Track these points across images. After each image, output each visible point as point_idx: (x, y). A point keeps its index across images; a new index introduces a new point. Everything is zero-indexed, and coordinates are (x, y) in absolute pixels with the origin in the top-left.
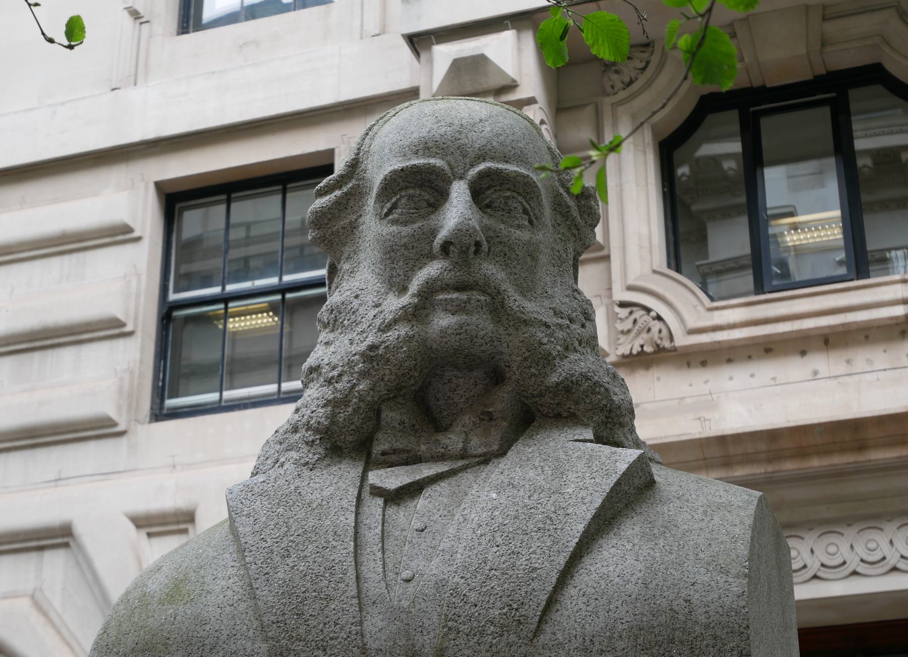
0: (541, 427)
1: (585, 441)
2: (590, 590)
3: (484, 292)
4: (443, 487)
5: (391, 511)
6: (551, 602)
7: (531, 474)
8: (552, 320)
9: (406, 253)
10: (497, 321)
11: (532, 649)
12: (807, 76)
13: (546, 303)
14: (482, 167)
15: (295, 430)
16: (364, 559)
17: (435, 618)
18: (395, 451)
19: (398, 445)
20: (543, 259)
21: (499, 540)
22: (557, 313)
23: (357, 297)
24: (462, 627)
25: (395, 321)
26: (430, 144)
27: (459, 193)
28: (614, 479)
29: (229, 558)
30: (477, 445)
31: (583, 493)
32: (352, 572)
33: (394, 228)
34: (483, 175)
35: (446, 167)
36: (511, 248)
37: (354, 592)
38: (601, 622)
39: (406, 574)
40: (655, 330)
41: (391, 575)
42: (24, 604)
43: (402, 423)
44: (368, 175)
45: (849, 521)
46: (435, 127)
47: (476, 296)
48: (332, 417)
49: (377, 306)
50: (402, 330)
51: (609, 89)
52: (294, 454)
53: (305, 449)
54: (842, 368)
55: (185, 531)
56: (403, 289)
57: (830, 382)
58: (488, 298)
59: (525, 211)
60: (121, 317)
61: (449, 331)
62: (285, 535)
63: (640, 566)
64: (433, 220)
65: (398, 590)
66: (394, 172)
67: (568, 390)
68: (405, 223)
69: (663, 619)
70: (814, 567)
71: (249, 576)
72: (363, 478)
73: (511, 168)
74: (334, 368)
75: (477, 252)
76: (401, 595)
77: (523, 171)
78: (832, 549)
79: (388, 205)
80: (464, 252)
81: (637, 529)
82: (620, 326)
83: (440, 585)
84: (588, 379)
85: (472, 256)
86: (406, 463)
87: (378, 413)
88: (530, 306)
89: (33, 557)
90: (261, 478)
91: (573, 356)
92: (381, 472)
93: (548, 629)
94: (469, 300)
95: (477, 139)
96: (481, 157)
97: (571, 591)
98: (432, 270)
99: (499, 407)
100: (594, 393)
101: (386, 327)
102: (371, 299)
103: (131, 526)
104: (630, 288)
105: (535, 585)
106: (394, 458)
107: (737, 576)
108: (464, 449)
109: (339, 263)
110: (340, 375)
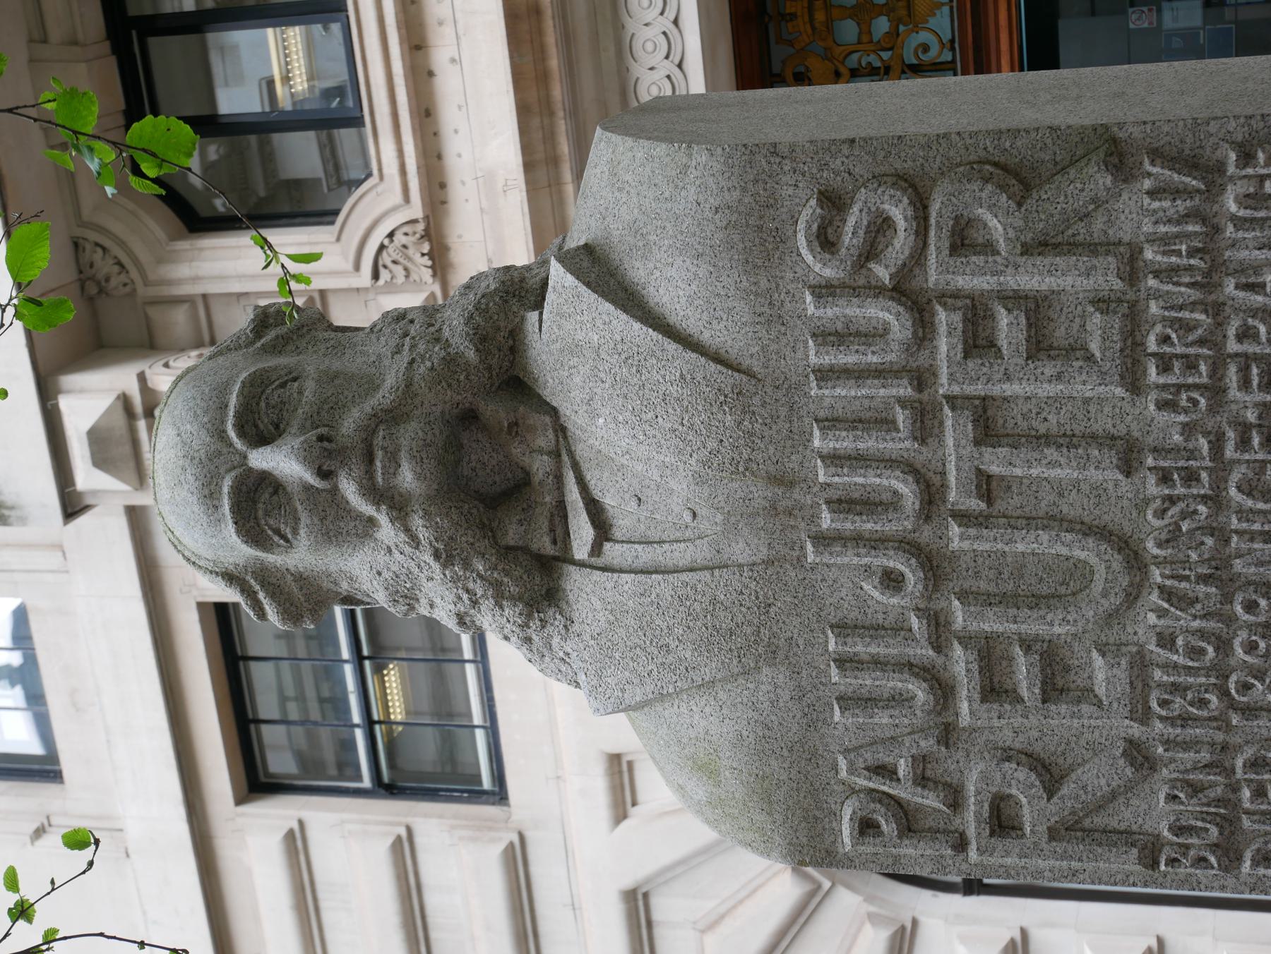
0: (525, 369)
1: (541, 321)
2: (705, 317)
3: (374, 431)
4: (591, 477)
5: (617, 533)
6: (717, 359)
7: (577, 380)
8: (405, 356)
9: (330, 518)
10: (406, 417)
11: (769, 380)
12: (112, 62)
13: (387, 362)
14: (232, 434)
15: (528, 640)
16: (670, 564)
17: (735, 485)
18: (552, 530)
19: (545, 526)
20: (336, 365)
21: (650, 415)
22: (398, 350)
23: (379, 574)
24: (745, 456)
25: (407, 530)
26: (206, 492)
27: (261, 459)
28: (583, 289)
29: (669, 711)
30: (545, 440)
31: (599, 323)
32: (685, 577)
33: (302, 532)
34: (242, 433)
35: (233, 474)
36: (325, 401)
37: (707, 574)
38: (740, 306)
39: (687, 517)
40: (404, 240)
41: (688, 534)
42: (709, 939)
43: (520, 522)
44: (241, 562)
45: (618, 26)
46: (186, 487)
47: (379, 440)
48: (514, 599)
49: (390, 551)
50: (417, 522)
51: (128, 289)
52: (556, 641)
53: (549, 629)
54: (448, 30)
55: (630, 764)
56: (371, 521)
58: (382, 427)
59: (283, 385)
60: (390, 840)
61: (419, 470)
62: (644, 650)
63: (679, 262)
64: (294, 489)
65: (704, 526)
66: (238, 532)
67: (484, 339)
68: (297, 520)
69: (736, 238)
70: (669, 67)
71: (690, 688)
72: (582, 564)
73: (233, 401)
74: (460, 598)
75: (329, 440)
76: (711, 522)
77: (237, 387)
78: (649, 46)
79: (276, 538)
80: (329, 454)
81: (637, 264)
82: (400, 278)
83: (699, 480)
84: (471, 317)
85: (333, 445)
86: (565, 517)
87: (509, 548)
88: (390, 381)
89: (658, 932)
90: (581, 678)
91: (446, 333)
92: (575, 545)
93: (747, 362)
94: (384, 449)
95: (201, 440)
96: (221, 435)
97: (706, 337)
98: (349, 489)
99: (502, 415)
100: (487, 310)
101: (414, 541)
102: (382, 558)
103: (625, 824)
104: (357, 267)
105: (699, 377)
106: (559, 531)
107: (690, 156)
108: (549, 453)
109: (341, 593)
110: (468, 591)
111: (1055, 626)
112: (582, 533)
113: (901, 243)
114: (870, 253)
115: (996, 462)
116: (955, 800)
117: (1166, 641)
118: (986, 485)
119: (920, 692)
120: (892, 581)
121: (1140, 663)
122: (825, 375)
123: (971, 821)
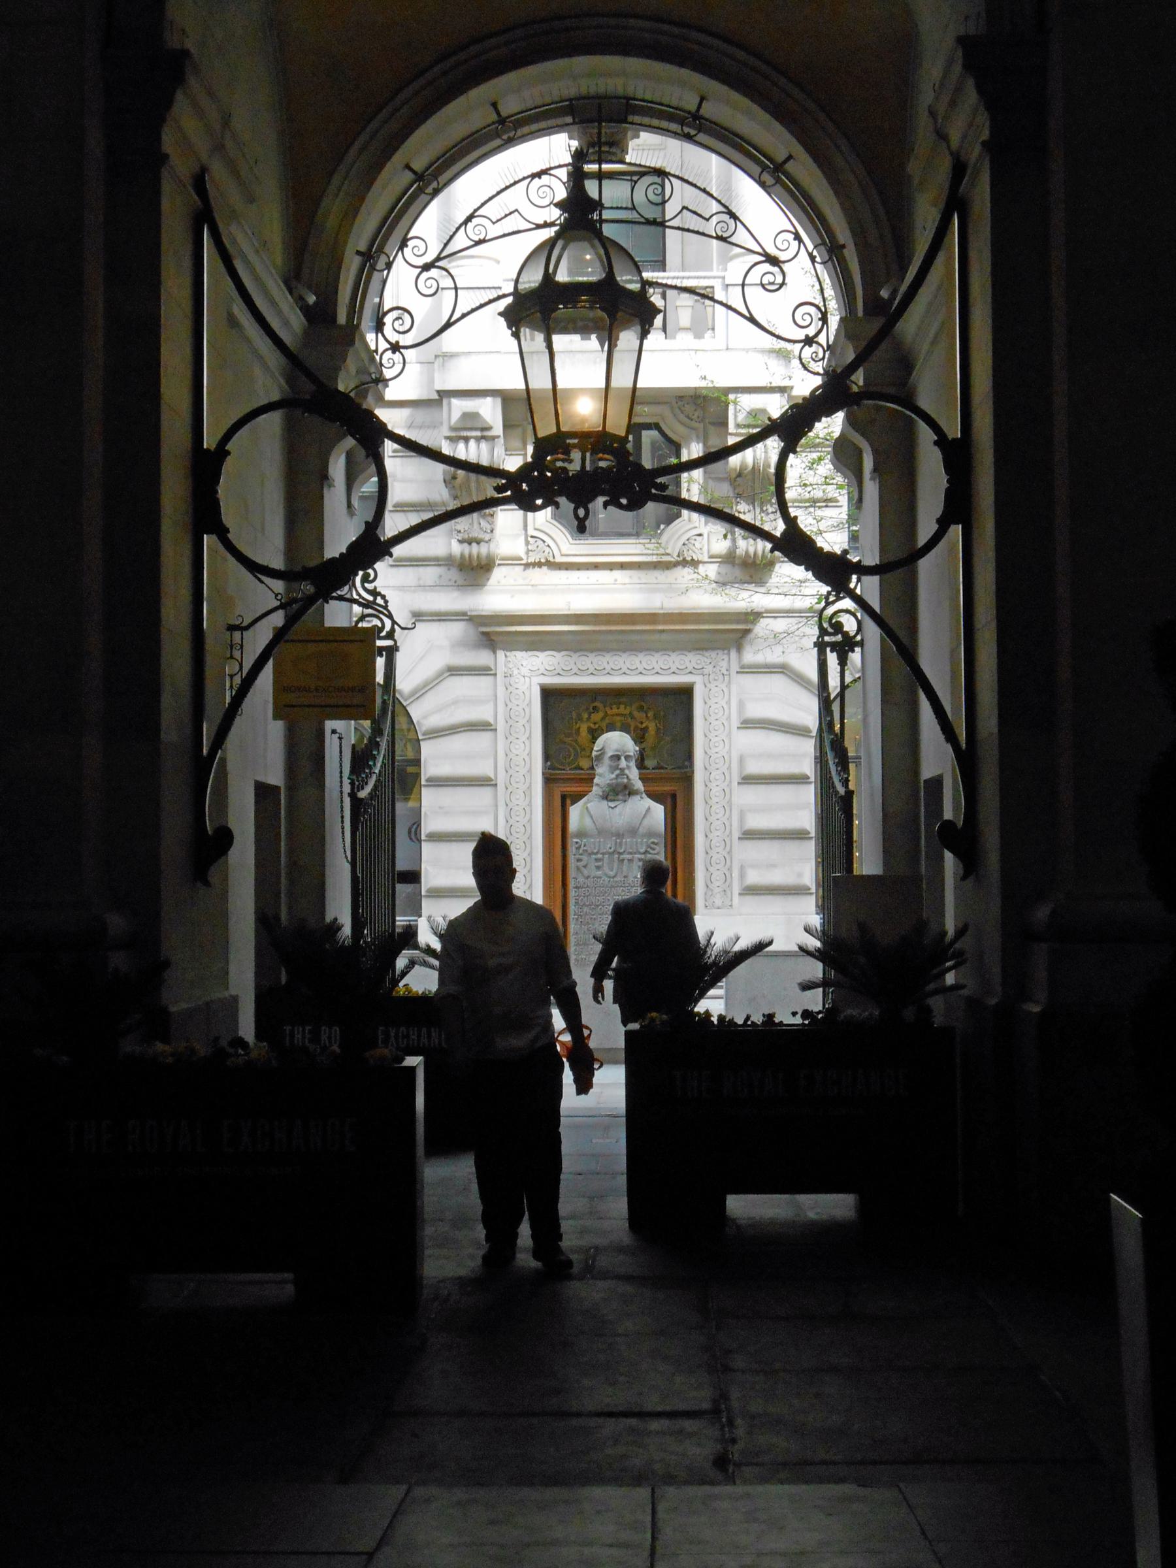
40: (546, 552)
57: (621, 586)
70: (608, 669)
104: (535, 529)
111: (606, 869)
112: (612, 804)
113: (651, 851)
114: (651, 848)
115: (626, 861)
116: (581, 855)
117: (604, 880)
118: (623, 860)
119: (595, 851)
120: (610, 848)
121: (600, 878)
122: (637, 842)
123: (577, 856)
